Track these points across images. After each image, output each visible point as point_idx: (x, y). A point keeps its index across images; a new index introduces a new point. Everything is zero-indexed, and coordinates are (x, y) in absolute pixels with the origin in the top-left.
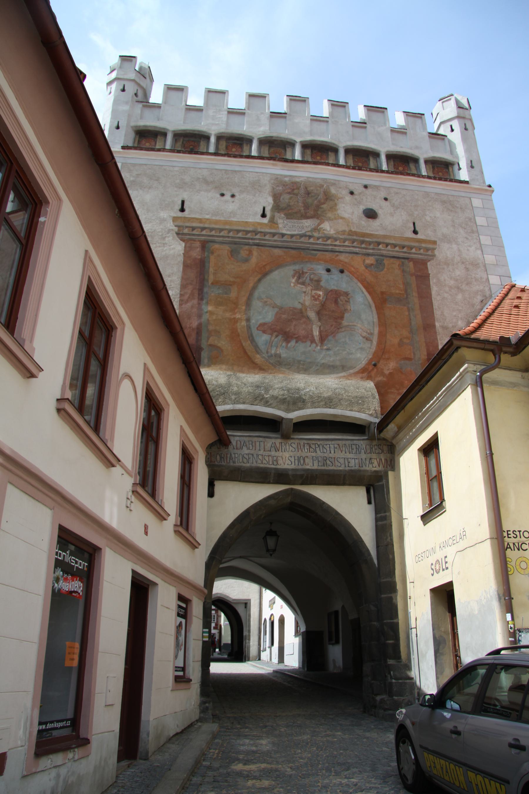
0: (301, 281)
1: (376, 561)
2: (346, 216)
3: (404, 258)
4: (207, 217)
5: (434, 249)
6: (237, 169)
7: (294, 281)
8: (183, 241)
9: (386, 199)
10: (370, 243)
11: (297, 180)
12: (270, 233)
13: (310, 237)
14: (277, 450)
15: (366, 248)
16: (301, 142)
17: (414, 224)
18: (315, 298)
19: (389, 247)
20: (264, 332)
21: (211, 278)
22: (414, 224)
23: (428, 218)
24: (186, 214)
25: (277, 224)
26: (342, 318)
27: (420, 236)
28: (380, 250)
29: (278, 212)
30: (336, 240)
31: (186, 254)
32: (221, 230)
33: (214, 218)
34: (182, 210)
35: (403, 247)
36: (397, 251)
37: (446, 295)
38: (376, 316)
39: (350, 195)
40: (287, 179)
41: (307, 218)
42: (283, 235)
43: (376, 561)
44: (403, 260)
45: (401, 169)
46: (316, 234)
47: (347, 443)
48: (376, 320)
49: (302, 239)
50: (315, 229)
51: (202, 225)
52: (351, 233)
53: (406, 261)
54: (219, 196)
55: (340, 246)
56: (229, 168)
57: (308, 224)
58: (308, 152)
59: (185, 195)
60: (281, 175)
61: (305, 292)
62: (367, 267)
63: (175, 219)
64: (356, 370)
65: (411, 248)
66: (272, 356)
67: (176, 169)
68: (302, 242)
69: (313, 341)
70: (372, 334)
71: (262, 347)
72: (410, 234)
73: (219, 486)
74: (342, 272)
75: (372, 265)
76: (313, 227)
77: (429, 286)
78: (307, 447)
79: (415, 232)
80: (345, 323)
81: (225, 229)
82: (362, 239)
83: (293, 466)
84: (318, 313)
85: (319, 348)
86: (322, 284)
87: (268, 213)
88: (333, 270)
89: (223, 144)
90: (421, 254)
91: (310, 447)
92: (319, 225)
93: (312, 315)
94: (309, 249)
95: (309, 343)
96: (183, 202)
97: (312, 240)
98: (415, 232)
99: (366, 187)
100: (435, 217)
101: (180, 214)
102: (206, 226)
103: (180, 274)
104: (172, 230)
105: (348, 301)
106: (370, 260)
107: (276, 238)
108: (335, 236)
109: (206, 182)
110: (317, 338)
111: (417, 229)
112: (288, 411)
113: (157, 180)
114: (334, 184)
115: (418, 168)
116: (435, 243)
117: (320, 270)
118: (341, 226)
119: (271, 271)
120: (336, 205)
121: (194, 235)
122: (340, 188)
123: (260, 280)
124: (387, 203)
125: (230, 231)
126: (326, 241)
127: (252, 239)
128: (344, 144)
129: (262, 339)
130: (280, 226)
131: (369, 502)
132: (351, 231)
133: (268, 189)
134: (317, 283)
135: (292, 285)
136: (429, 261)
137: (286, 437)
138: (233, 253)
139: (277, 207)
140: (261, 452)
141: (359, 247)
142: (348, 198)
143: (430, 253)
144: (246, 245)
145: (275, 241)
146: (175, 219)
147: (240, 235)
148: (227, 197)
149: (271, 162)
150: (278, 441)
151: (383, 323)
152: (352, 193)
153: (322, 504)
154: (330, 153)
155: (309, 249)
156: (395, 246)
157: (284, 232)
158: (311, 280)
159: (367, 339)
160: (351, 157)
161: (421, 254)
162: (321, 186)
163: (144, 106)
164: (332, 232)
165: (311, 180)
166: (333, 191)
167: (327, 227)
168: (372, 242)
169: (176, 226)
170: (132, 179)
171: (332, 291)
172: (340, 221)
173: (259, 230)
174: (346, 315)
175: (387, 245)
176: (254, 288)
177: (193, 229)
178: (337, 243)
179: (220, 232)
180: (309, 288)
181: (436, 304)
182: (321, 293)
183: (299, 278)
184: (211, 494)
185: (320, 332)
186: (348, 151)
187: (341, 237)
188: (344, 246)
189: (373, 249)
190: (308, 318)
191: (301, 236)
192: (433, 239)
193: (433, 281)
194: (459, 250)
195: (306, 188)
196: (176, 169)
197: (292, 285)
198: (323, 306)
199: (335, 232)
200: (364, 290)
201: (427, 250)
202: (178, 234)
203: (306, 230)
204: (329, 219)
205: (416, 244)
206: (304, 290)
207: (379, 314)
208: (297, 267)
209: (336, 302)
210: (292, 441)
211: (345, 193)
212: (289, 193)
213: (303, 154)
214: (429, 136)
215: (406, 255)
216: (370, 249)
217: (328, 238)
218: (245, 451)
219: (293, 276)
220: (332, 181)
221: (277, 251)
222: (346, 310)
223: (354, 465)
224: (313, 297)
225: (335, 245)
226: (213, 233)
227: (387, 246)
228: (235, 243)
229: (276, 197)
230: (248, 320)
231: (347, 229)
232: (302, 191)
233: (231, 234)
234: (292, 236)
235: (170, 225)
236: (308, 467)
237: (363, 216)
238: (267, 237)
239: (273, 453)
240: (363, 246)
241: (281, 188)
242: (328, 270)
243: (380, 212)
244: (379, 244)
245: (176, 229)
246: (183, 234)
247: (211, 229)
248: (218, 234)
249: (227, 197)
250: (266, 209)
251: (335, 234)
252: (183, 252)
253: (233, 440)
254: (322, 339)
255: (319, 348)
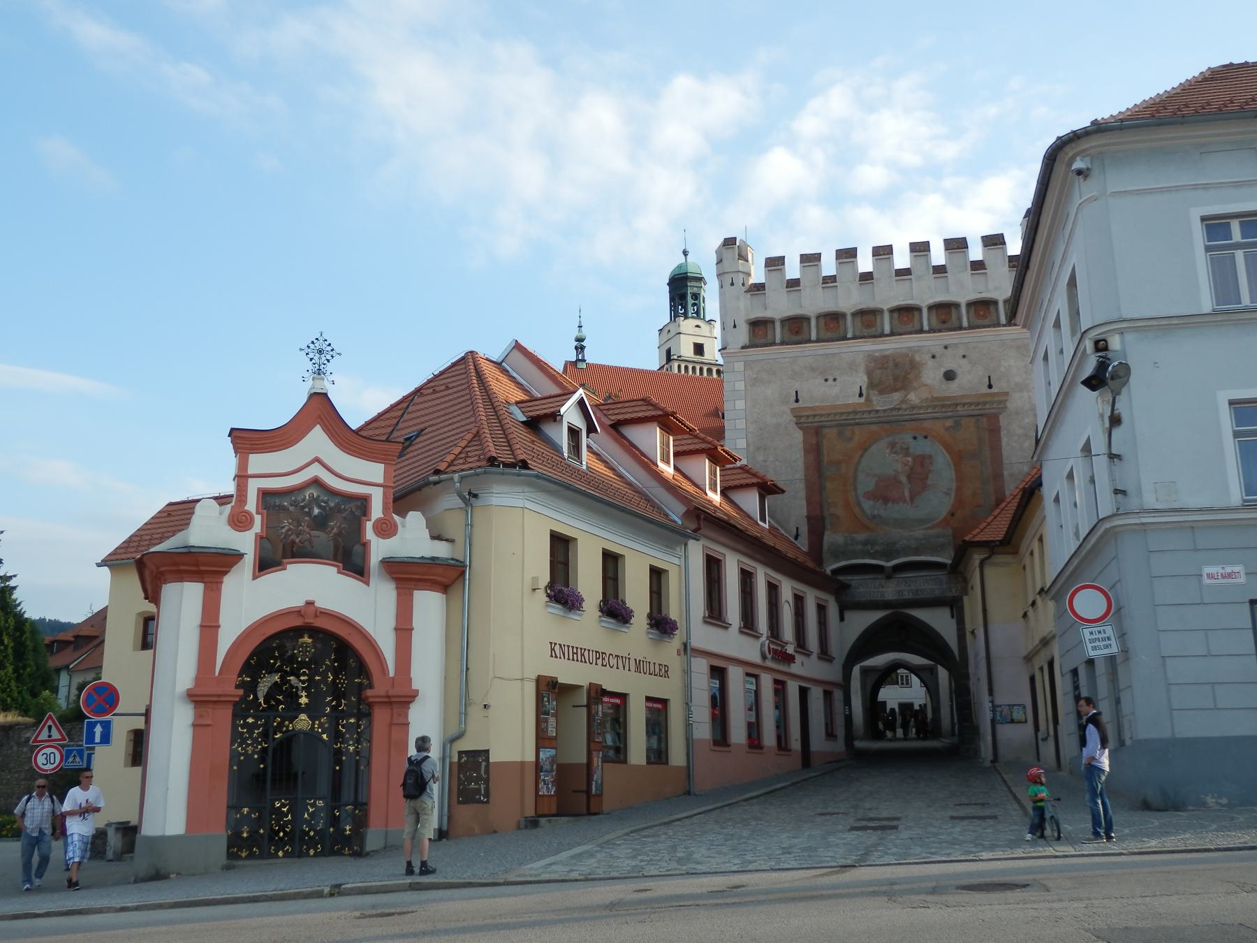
0: (894, 450)
1: (958, 658)
2: (929, 382)
3: (979, 415)
4: (817, 404)
5: (1006, 400)
6: (836, 351)
7: (888, 451)
8: (801, 428)
9: (964, 357)
10: (949, 406)
11: (887, 353)
12: (867, 411)
13: (899, 409)
14: (883, 587)
15: (945, 412)
16: (888, 309)
17: (989, 377)
18: (905, 464)
19: (966, 406)
20: (868, 499)
21: (826, 459)
22: (989, 377)
23: (1002, 369)
24: (801, 404)
25: (872, 402)
26: (927, 478)
27: (994, 390)
28: (957, 411)
29: (873, 390)
30: (920, 408)
31: (804, 441)
32: (829, 415)
33: (822, 404)
34: (797, 401)
35: (978, 405)
36: (973, 410)
37: (1014, 444)
38: (953, 473)
39: (932, 359)
40: (877, 354)
41: (897, 390)
42: (877, 411)
43: (958, 658)
44: (978, 417)
45: (982, 313)
46: (904, 406)
47: (933, 577)
48: (954, 477)
49: (894, 413)
50: (902, 402)
51: (813, 413)
52: (934, 399)
53: (980, 417)
54: (823, 381)
55: (923, 414)
56: (829, 351)
57: (897, 396)
58: (896, 315)
59: (797, 386)
60: (872, 351)
61: (897, 460)
62: (947, 429)
63: (793, 410)
64: (938, 520)
65: (985, 403)
66: (874, 517)
67: (788, 360)
68: (893, 416)
69: (905, 501)
70: (950, 489)
71: (868, 512)
72: (985, 390)
73: (849, 615)
74: (926, 437)
75: (951, 427)
76: (901, 399)
77: (999, 440)
78: (904, 583)
79: (990, 386)
80: (929, 482)
81: (831, 414)
82: (942, 403)
83: (895, 598)
84: (909, 477)
85: (909, 506)
86: (911, 450)
87: (864, 392)
88: (918, 438)
89: (822, 321)
90: (993, 408)
91: (906, 583)
92: (906, 396)
93: (903, 479)
94: (899, 421)
95: (901, 504)
96: (797, 392)
97: (901, 412)
98: (990, 386)
99: (946, 347)
100: (1009, 366)
101: (796, 405)
102: (818, 413)
103: (803, 459)
104: (791, 420)
105: (931, 463)
106: (949, 423)
107: (872, 415)
108: (919, 405)
109: (813, 369)
110: (908, 499)
111: (992, 383)
112: (888, 561)
113: (774, 374)
114: (918, 351)
115: (997, 310)
116: (1007, 394)
117: (908, 438)
118: (925, 394)
119: (870, 446)
120: (920, 372)
121: (809, 423)
122: (923, 353)
123: (862, 456)
124: (964, 361)
125: (835, 414)
126: (912, 411)
127: (855, 419)
128: (926, 304)
129: (867, 505)
130: (875, 403)
131: (953, 617)
132: (933, 397)
133: (862, 368)
134: (906, 451)
135: (887, 455)
136: (1001, 414)
137: (889, 577)
138: (840, 434)
139: (872, 385)
140: (872, 589)
141: (939, 412)
142: (931, 363)
143: (1001, 406)
144: (848, 425)
145: (871, 418)
146: (793, 410)
147: (844, 417)
148: (830, 382)
149: (863, 340)
150: (883, 581)
151: (960, 477)
152: (934, 357)
153: (918, 620)
154: (915, 313)
155: (899, 421)
156: (971, 404)
157: (879, 408)
158: (902, 448)
159: (947, 494)
160: (934, 312)
161: (993, 408)
162: (907, 355)
163: (751, 295)
164: (917, 401)
165: (898, 350)
166: (917, 358)
167: (913, 397)
168: (951, 404)
169: (794, 417)
170: (755, 376)
171: (918, 456)
172: (925, 388)
173: (859, 410)
174: (930, 476)
175: (964, 405)
176: (858, 463)
177: (808, 417)
178: (922, 411)
179: (828, 417)
180: (901, 456)
181: (1005, 453)
182: (910, 459)
183: (892, 448)
184: (842, 619)
185: (910, 492)
186: (932, 308)
187: (925, 405)
188: (927, 413)
189: (952, 411)
190: (900, 482)
191: (892, 409)
192: (1006, 391)
193: (1003, 433)
194: (1030, 398)
195: (894, 360)
196: (788, 360)
197: (887, 455)
198: (912, 469)
199: (919, 401)
200: (944, 450)
201: (1000, 402)
202: (797, 424)
203: (895, 403)
204: (915, 389)
205: (988, 399)
206: (897, 458)
207: (956, 471)
208: (890, 439)
209: (922, 465)
210: (892, 580)
211: (927, 357)
212: (880, 368)
213: (891, 318)
214: (1009, 271)
215: (980, 412)
216: (949, 412)
217: (914, 408)
218: (861, 590)
219: (888, 447)
220: (916, 348)
221: (874, 427)
222: (930, 471)
223: (937, 593)
224: (904, 463)
225: (920, 414)
226: (823, 419)
227: (964, 406)
228: (841, 425)
229: (869, 374)
230: (855, 489)
231: (929, 396)
232: (891, 364)
233: (837, 418)
234: (885, 411)
235: (789, 418)
236: (905, 597)
237: (943, 379)
238: (865, 416)
239: (881, 590)
240: (944, 410)
241: (873, 365)
242: (915, 438)
243: (959, 371)
244: (957, 405)
245: (795, 419)
246: (801, 423)
247: (821, 415)
248: (827, 419)
249: (830, 382)
250: (862, 388)
251: (919, 403)
252: (802, 439)
253: (853, 583)
254: (912, 499)
255: (909, 506)
